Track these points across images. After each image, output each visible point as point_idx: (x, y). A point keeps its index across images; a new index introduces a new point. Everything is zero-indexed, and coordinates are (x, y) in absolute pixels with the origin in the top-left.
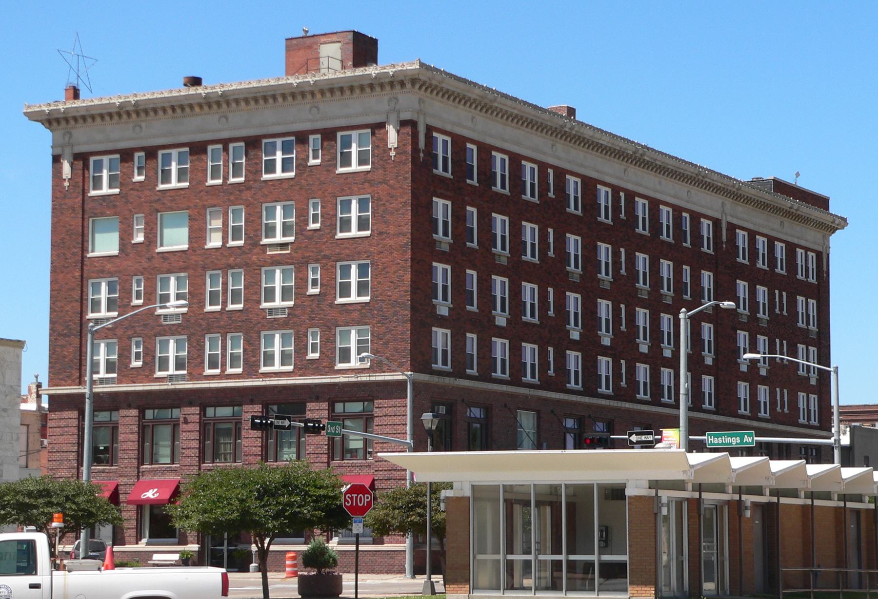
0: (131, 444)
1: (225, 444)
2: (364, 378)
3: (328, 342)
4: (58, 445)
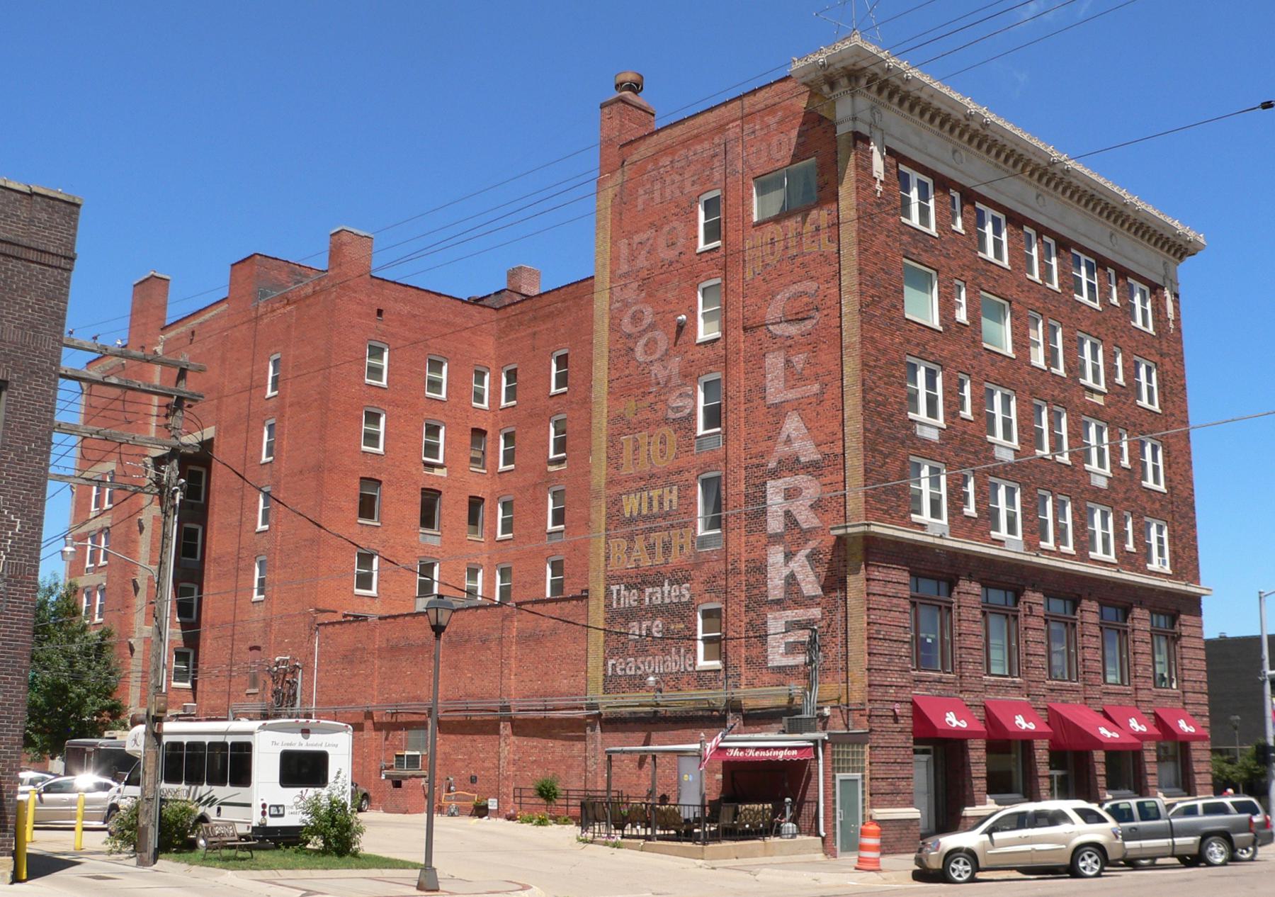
0: (974, 638)
2: (1167, 584)
4: (885, 628)
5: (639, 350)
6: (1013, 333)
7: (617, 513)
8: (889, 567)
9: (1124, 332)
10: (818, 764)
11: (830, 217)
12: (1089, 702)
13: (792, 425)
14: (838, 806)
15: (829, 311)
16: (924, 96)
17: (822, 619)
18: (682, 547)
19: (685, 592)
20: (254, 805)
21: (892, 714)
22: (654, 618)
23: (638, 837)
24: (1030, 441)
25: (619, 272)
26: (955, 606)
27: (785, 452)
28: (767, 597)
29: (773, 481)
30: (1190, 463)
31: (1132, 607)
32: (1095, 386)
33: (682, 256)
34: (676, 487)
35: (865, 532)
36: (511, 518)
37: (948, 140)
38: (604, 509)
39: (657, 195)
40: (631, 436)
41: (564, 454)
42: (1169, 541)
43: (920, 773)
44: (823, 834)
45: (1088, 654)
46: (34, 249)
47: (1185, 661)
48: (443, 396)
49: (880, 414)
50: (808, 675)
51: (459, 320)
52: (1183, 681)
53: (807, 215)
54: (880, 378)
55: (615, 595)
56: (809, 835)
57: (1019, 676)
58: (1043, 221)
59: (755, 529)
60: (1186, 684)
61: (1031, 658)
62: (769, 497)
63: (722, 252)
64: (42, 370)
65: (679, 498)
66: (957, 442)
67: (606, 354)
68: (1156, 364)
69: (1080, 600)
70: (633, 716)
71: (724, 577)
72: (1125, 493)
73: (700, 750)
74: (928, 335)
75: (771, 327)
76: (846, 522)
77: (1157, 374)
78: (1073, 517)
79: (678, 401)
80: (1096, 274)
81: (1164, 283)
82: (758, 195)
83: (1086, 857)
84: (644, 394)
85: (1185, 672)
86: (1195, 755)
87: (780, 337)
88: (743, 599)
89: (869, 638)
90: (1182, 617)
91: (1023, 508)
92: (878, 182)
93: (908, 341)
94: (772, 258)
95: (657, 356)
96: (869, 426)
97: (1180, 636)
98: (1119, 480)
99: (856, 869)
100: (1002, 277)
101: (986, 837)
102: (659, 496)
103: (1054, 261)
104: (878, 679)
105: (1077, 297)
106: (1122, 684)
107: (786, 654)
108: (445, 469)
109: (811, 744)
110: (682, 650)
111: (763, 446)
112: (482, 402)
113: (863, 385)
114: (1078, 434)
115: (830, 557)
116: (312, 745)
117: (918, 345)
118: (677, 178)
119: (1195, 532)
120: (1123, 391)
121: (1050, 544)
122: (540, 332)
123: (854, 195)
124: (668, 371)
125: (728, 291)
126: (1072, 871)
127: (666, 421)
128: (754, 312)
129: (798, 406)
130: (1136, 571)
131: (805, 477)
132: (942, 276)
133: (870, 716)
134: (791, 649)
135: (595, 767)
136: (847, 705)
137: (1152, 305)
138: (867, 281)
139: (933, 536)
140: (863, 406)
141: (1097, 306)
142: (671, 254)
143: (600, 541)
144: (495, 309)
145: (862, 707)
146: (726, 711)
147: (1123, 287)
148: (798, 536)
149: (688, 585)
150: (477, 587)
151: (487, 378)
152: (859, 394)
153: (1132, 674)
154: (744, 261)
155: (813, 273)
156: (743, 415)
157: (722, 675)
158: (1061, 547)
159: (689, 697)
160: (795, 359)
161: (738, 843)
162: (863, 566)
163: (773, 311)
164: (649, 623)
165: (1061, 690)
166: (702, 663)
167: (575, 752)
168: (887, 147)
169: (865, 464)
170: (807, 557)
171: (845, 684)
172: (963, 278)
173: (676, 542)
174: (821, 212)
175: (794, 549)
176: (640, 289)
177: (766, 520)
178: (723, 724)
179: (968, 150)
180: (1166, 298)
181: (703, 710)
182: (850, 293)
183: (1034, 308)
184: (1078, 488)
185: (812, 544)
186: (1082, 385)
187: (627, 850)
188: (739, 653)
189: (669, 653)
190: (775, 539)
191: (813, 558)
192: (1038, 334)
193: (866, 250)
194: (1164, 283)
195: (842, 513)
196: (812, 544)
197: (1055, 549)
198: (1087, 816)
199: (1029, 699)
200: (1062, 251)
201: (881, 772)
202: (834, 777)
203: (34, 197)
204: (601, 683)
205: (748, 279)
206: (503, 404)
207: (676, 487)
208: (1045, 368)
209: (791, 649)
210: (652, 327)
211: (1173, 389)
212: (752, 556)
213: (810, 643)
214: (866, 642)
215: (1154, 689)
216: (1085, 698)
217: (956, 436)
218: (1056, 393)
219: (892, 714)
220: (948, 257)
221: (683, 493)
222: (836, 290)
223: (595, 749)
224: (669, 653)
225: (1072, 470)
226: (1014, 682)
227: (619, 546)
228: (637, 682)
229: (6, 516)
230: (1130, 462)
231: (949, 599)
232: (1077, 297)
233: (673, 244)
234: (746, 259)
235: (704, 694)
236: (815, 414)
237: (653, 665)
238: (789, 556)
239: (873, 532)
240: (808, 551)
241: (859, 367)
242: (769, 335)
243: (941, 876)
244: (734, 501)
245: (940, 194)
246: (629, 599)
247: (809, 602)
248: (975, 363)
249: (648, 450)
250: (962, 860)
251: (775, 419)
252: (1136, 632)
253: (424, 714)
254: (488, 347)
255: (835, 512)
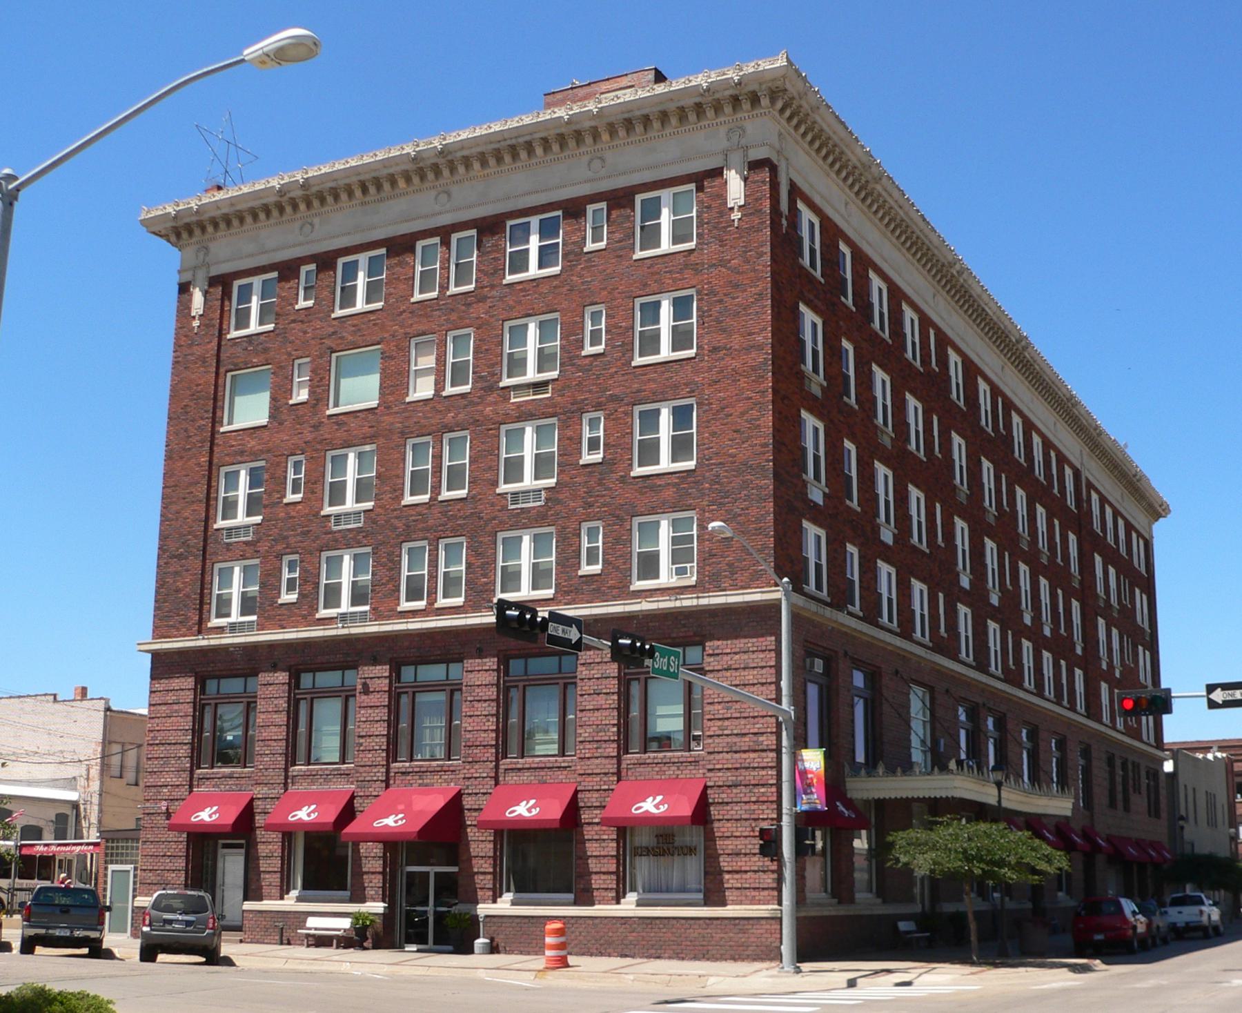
0: (274, 729)
1: (432, 728)
2: (688, 602)
3: (618, 544)
4: (162, 734)
202: (106, 869)
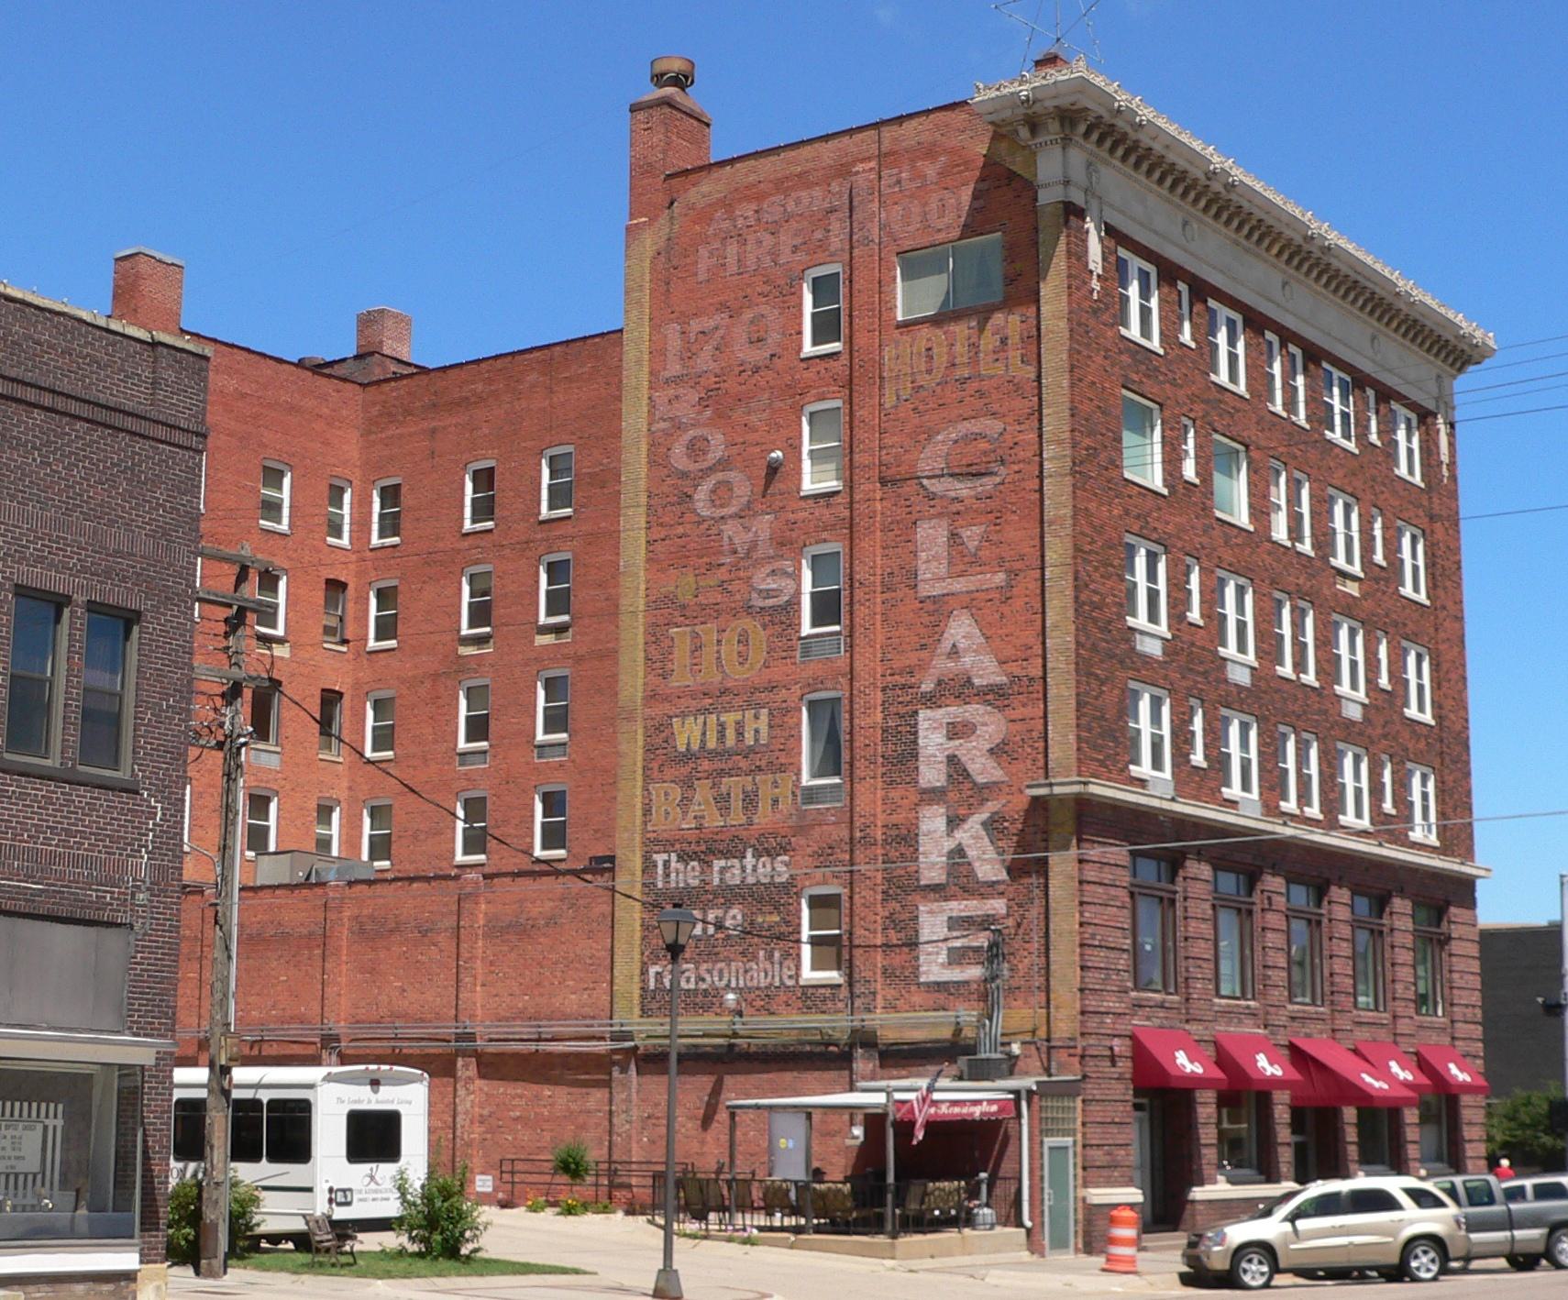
4: (1102, 931)
5: (702, 494)
6: (1250, 494)
7: (665, 745)
8: (1094, 842)
9: (1384, 485)
10: (1020, 1125)
11: (1024, 326)
12: (1338, 1035)
13: (961, 630)
14: (1046, 1185)
15: (1021, 466)
16: (1158, 147)
17: (1008, 915)
18: (776, 801)
19: (781, 869)
20: (317, 1190)
21: (1108, 1053)
22: (728, 905)
23: (782, 1229)
24: (1269, 654)
25: (667, 374)
26: (1179, 897)
27: (949, 669)
28: (918, 880)
29: (928, 711)
30: (1464, 678)
31: (1390, 896)
32: (1347, 568)
33: (775, 359)
34: (765, 711)
35: (1079, 794)
36: (393, 726)
37: (1178, 206)
38: (640, 738)
39: (731, 260)
40: (689, 629)
41: (488, 629)
42: (1437, 797)
43: (1132, 1140)
44: (1028, 1224)
45: (1338, 966)
46: (164, 424)
47: (1456, 976)
48: (284, 526)
49: (1095, 620)
50: (985, 995)
51: (309, 403)
52: (1452, 1005)
53: (987, 319)
54: (1096, 569)
55: (660, 870)
56: (1005, 1226)
57: (1254, 998)
58: (1289, 322)
59: (899, 780)
60: (1455, 1009)
61: (1270, 973)
62: (921, 733)
63: (844, 360)
64: (177, 595)
65: (771, 727)
66: (1183, 658)
67: (643, 499)
68: (1423, 531)
69: (1328, 887)
70: (693, 1050)
71: (847, 848)
72: (1384, 727)
73: (886, 1106)
74: (1150, 500)
75: (925, 482)
76: (1047, 778)
77: (1425, 545)
78: (1320, 765)
79: (769, 580)
80: (1351, 398)
81: (1438, 407)
82: (903, 280)
83: (1420, 1254)
84: (710, 567)
85: (1455, 991)
86: (1467, 1114)
87: (942, 497)
88: (879, 881)
89: (1082, 945)
90: (1453, 910)
91: (1260, 753)
92: (1095, 277)
93: (1127, 512)
94: (928, 377)
95: (732, 510)
96: (1083, 639)
97: (1449, 938)
98: (1377, 708)
99: (1104, 1270)
100: (1238, 411)
101: (1288, 1227)
102: (737, 723)
103: (1300, 381)
104: (1092, 1003)
105: (1328, 434)
106: (1377, 1009)
107: (950, 964)
108: (287, 645)
109: (1011, 1096)
110: (777, 955)
111: (911, 659)
112: (339, 535)
113: (1076, 579)
114: (1326, 642)
115: (1020, 826)
116: (382, 1102)
117: (1138, 517)
118: (768, 240)
119: (1469, 783)
120: (1383, 574)
121: (1290, 805)
122: (444, 428)
123: (1065, 298)
124: (751, 535)
125: (856, 422)
126: (1398, 1272)
127: (749, 609)
128: (897, 456)
129: (971, 603)
130: (1396, 843)
131: (981, 708)
132: (1167, 413)
133: (1083, 1057)
134: (958, 957)
135: (627, 1126)
136: (1048, 1040)
137: (1421, 441)
138: (1082, 425)
139: (1161, 798)
140: (1076, 610)
141: (1351, 446)
142: (757, 355)
143: (634, 787)
144: (360, 384)
145: (1072, 1044)
146: (852, 1046)
147: (1386, 415)
148: (969, 793)
149: (786, 858)
150: (331, 836)
151: (347, 497)
152: (1070, 592)
153: (1389, 996)
154: (881, 378)
155: (996, 407)
156: (878, 609)
157: (844, 993)
158: (1306, 809)
159: (789, 1024)
160: (966, 533)
161: (930, 1236)
162: (1074, 841)
163: (930, 459)
164: (720, 913)
165: (1304, 1019)
166: (808, 974)
167: (591, 1104)
168: (1106, 224)
169: (1078, 695)
170: (984, 824)
171: (1044, 1011)
172: (1191, 415)
173: (766, 793)
174: (1011, 318)
175: (962, 811)
176: (703, 403)
177: (917, 768)
178: (845, 1065)
179: (1201, 221)
180: (1438, 431)
181: (810, 1043)
182: (1060, 442)
183: (1277, 454)
184: (1327, 721)
185: (992, 806)
186: (1333, 568)
187: (766, 1248)
188: (872, 965)
189: (755, 958)
190: (932, 796)
191: (994, 826)
192: (1280, 494)
193: (1080, 380)
194: (1438, 407)
195: (1041, 763)
196: (992, 806)
197: (1297, 812)
198: (1421, 1198)
199: (1267, 1032)
200: (1312, 367)
201: (1096, 1136)
203: (160, 349)
204: (636, 1000)
205: (887, 406)
206: (375, 541)
207: (765, 711)
208: (1289, 544)
209: (958, 957)
210: (724, 464)
211: (1443, 571)
212: (895, 819)
213: (990, 947)
214: (1078, 950)
215: (1416, 1017)
216: (1333, 1031)
217: (1182, 649)
218: (1301, 581)
219: (1108, 1053)
220: (1173, 383)
221: (778, 721)
222: (1033, 436)
223: (628, 1100)
224: (755, 958)
225: (1320, 695)
226: (1248, 1007)
227: (666, 794)
228: (706, 1000)
229: (145, 800)
230: (1390, 680)
231: (1171, 887)
232: (1328, 434)
233: (759, 341)
234: (885, 374)
235: (815, 1020)
236: (997, 616)
237: (726, 975)
238: (954, 822)
239: (1093, 794)
240: (985, 816)
241: (1070, 552)
242: (925, 493)
243: (1229, 1279)
244: (866, 737)
245: (1166, 289)
246: (686, 875)
247: (989, 890)
248: (1205, 540)
249: (718, 652)
250: (1256, 1258)
251: (932, 619)
252: (1396, 933)
253: (315, 1043)
254: (350, 447)
255: (1029, 762)
